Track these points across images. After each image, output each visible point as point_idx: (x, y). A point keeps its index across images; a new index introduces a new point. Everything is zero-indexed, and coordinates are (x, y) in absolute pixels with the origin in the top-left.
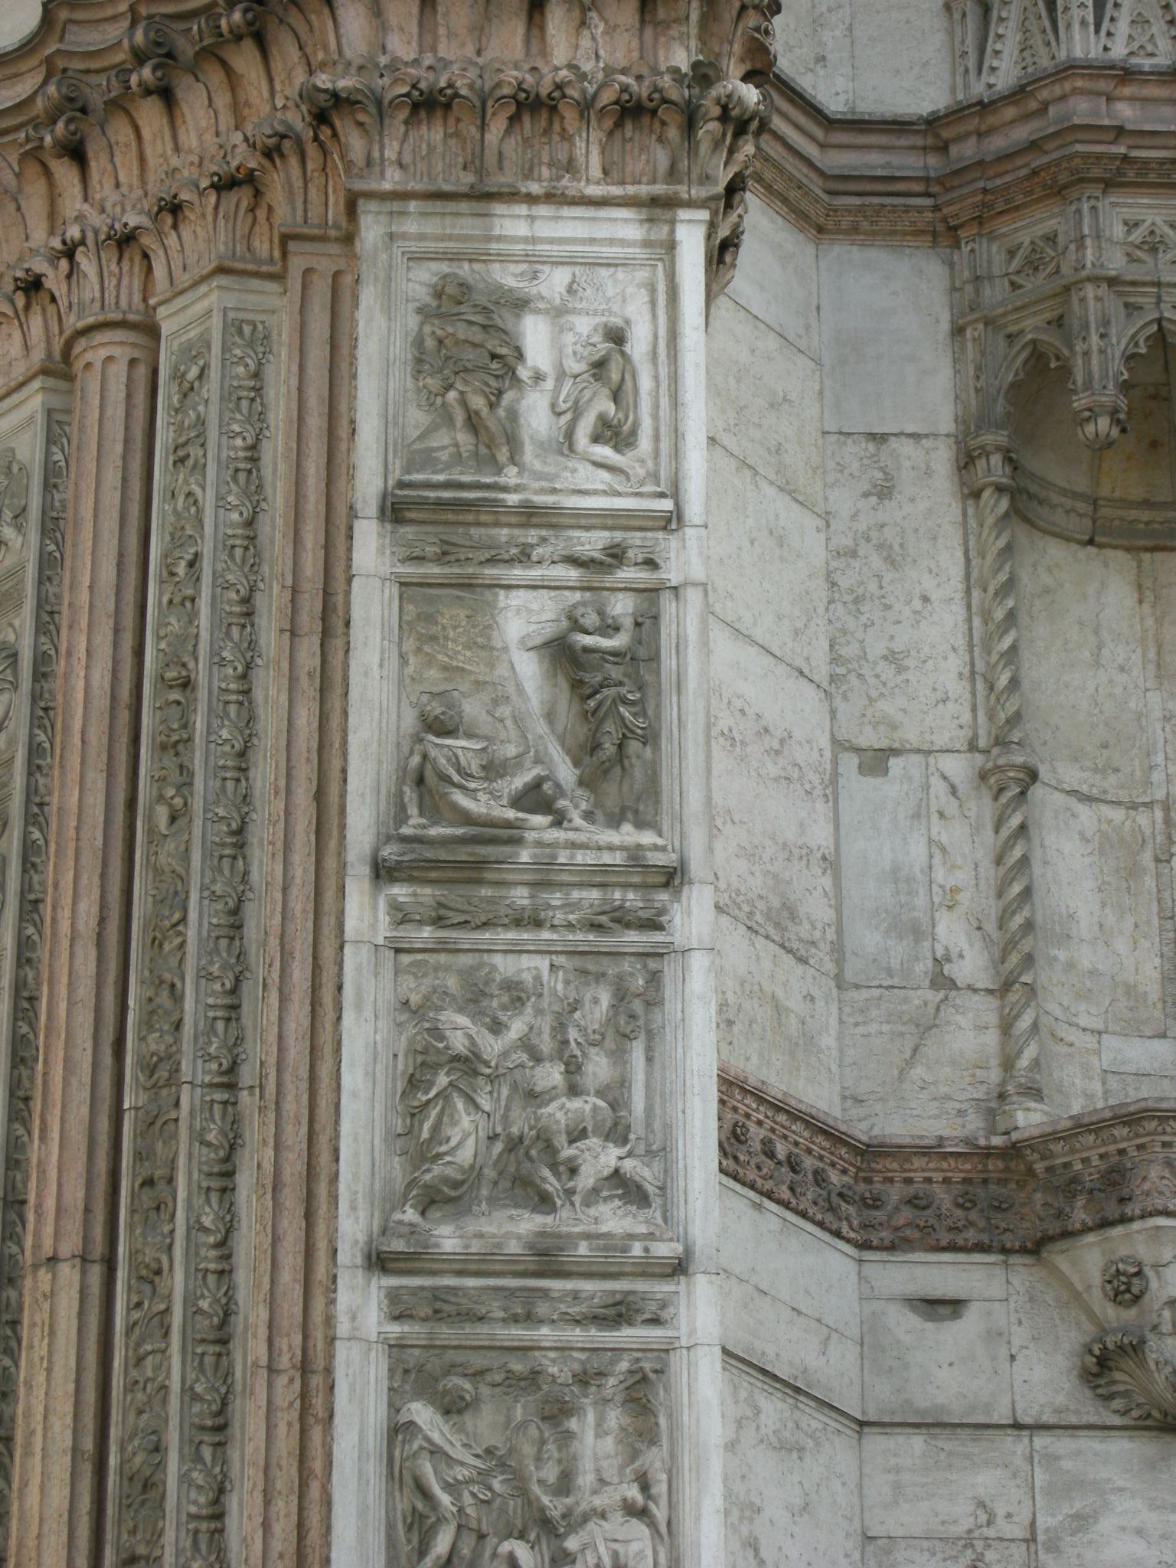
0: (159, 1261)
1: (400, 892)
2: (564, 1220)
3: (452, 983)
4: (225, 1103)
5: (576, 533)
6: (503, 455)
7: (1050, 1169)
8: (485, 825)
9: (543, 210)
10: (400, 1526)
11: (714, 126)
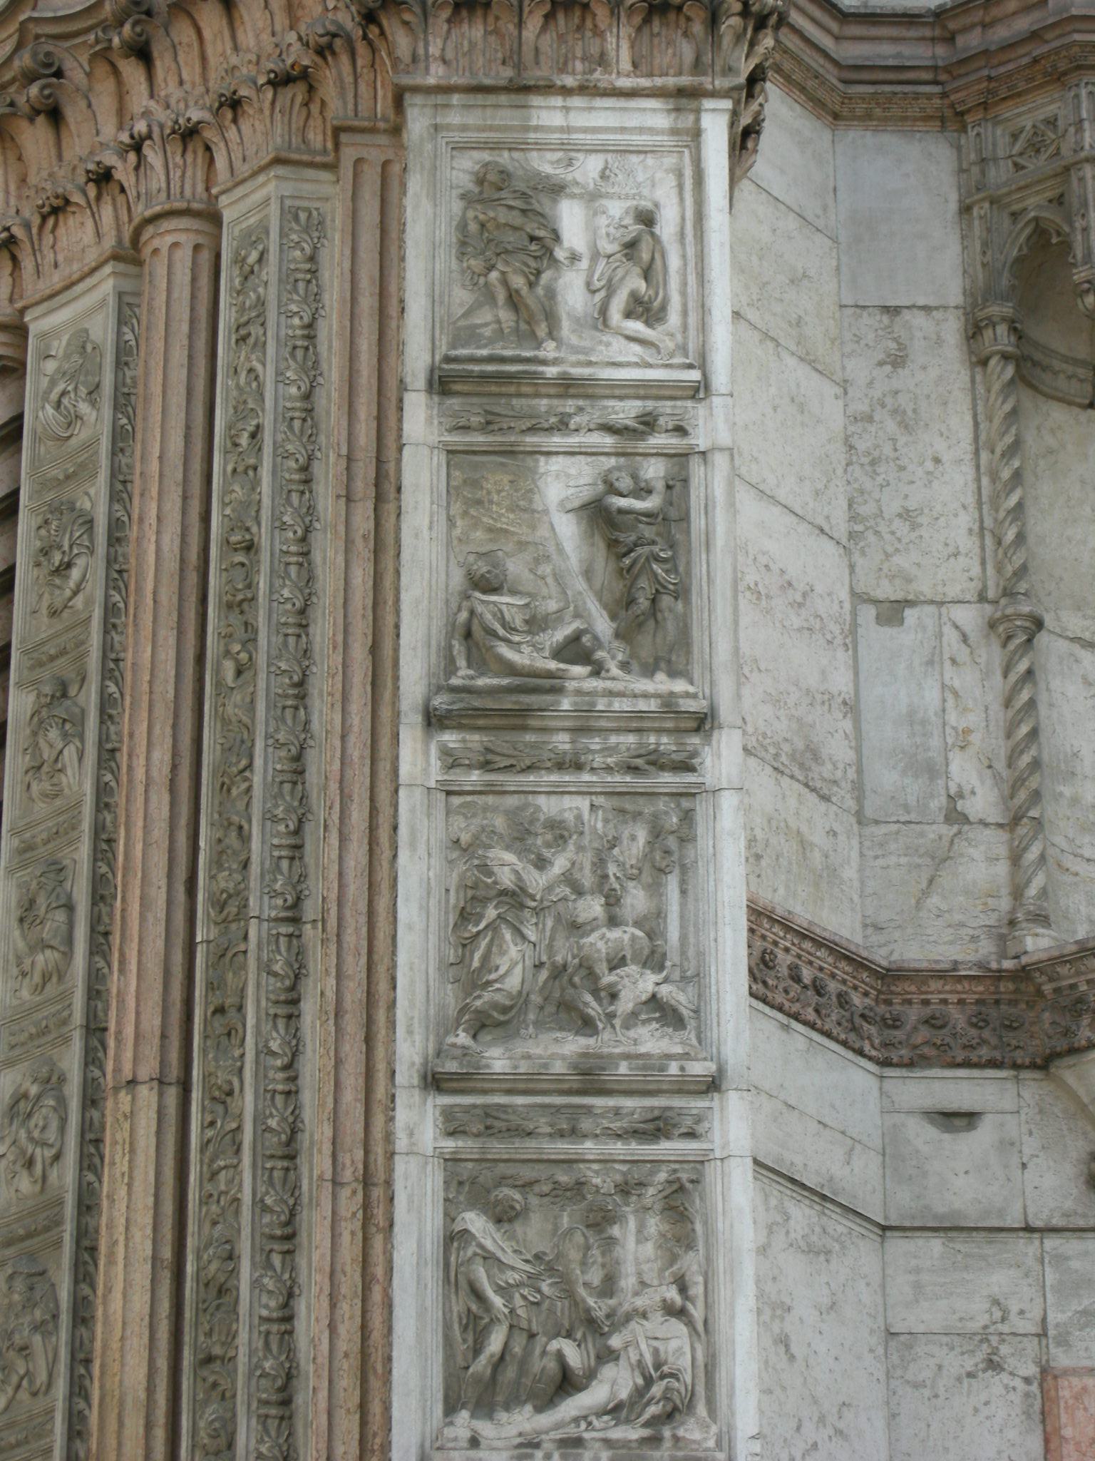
0: (230, 1083)
1: (451, 738)
2: (606, 1042)
3: (499, 822)
4: (290, 936)
5: (611, 403)
6: (542, 331)
7: (1057, 991)
9: (577, 101)
10: (456, 1326)
11: (735, 21)
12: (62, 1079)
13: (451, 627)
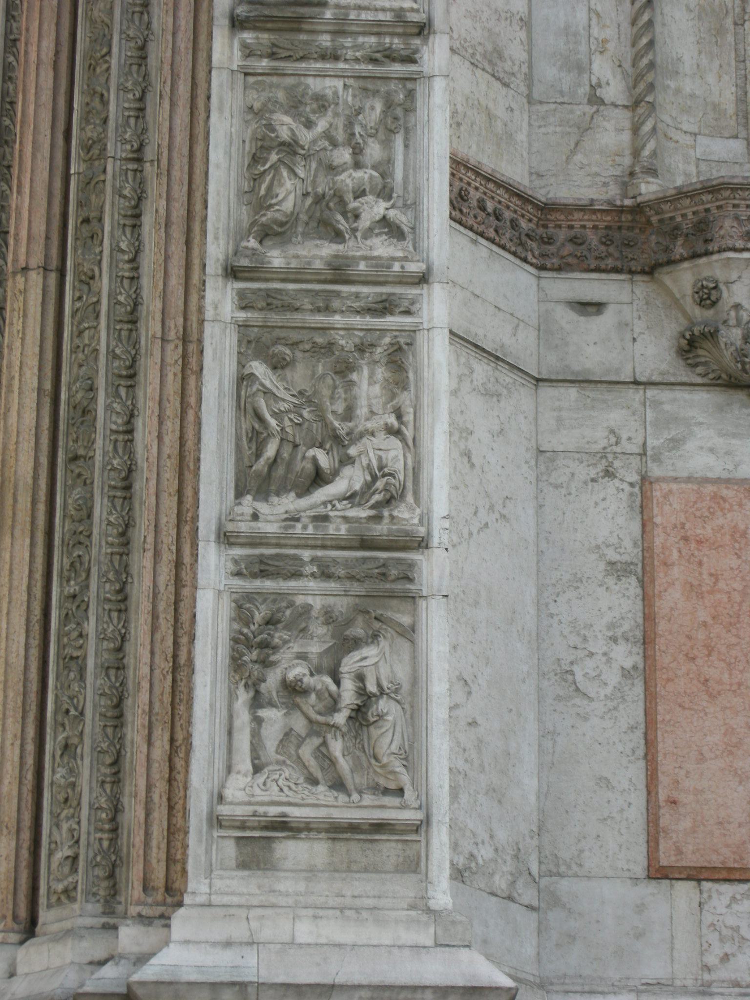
0: (93, 271)
1: (248, 36)
2: (351, 248)
3: (281, 95)
4: (135, 171)
7: (661, 221)
10: (244, 438)
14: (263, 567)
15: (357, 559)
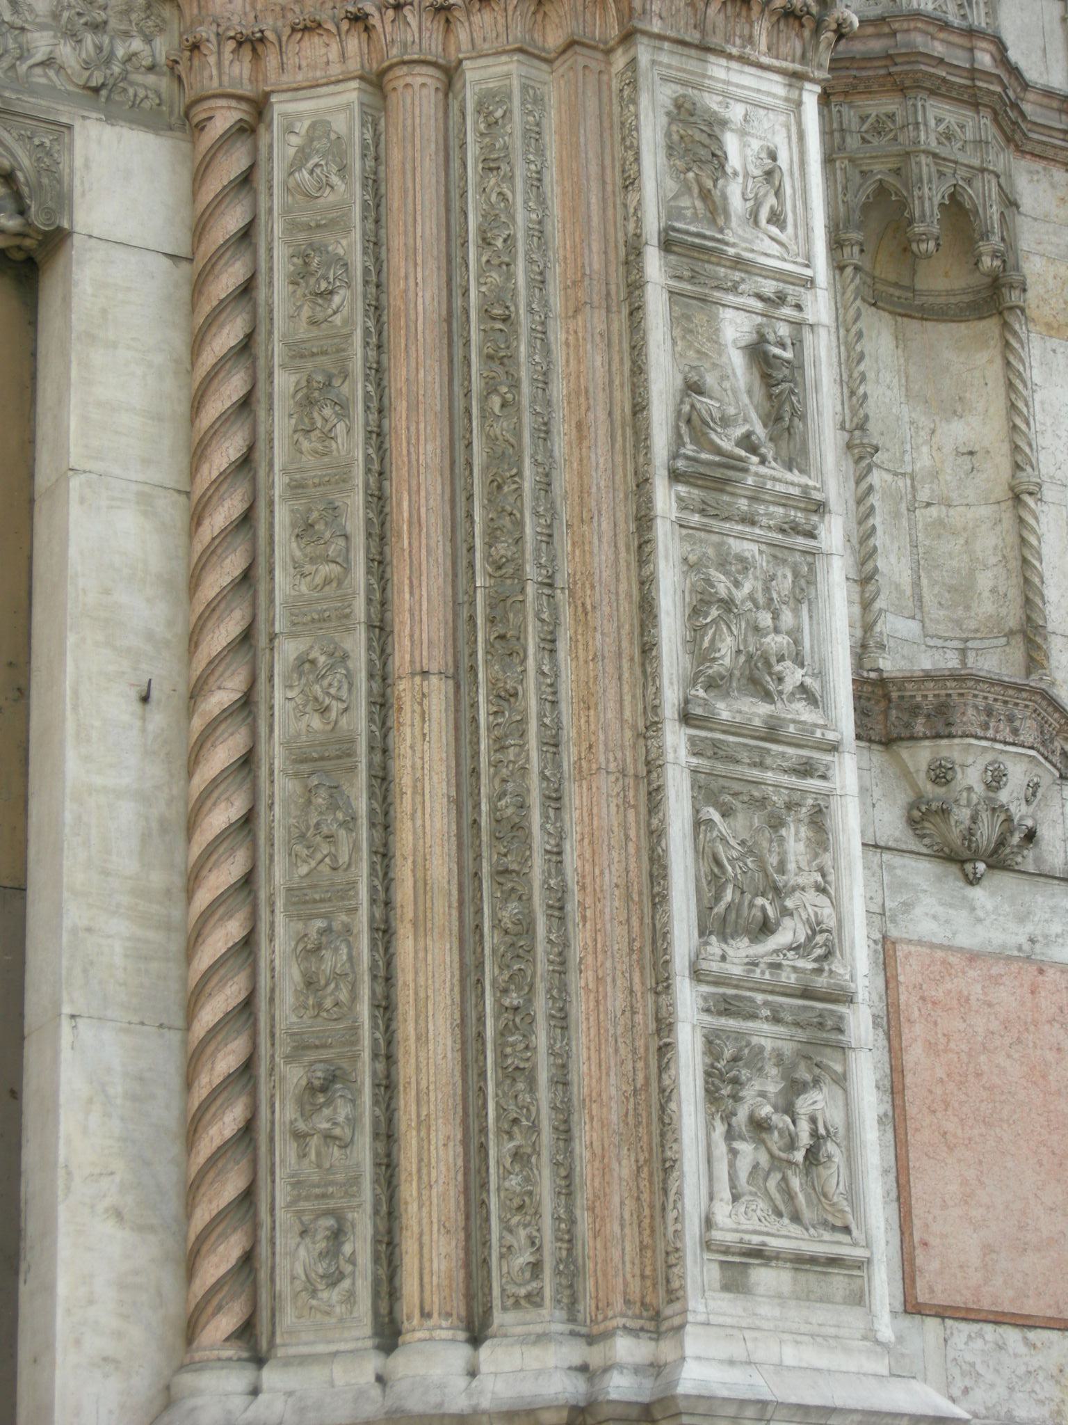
0: (515, 689)
1: (682, 489)
3: (711, 552)
4: (549, 596)
5: (759, 279)
6: (721, 221)
7: (901, 698)
8: (728, 457)
9: (735, 65)
10: (704, 880)
11: (830, 35)
12: (345, 657)
13: (679, 413)
14: (728, 1007)
15: (799, 1007)
